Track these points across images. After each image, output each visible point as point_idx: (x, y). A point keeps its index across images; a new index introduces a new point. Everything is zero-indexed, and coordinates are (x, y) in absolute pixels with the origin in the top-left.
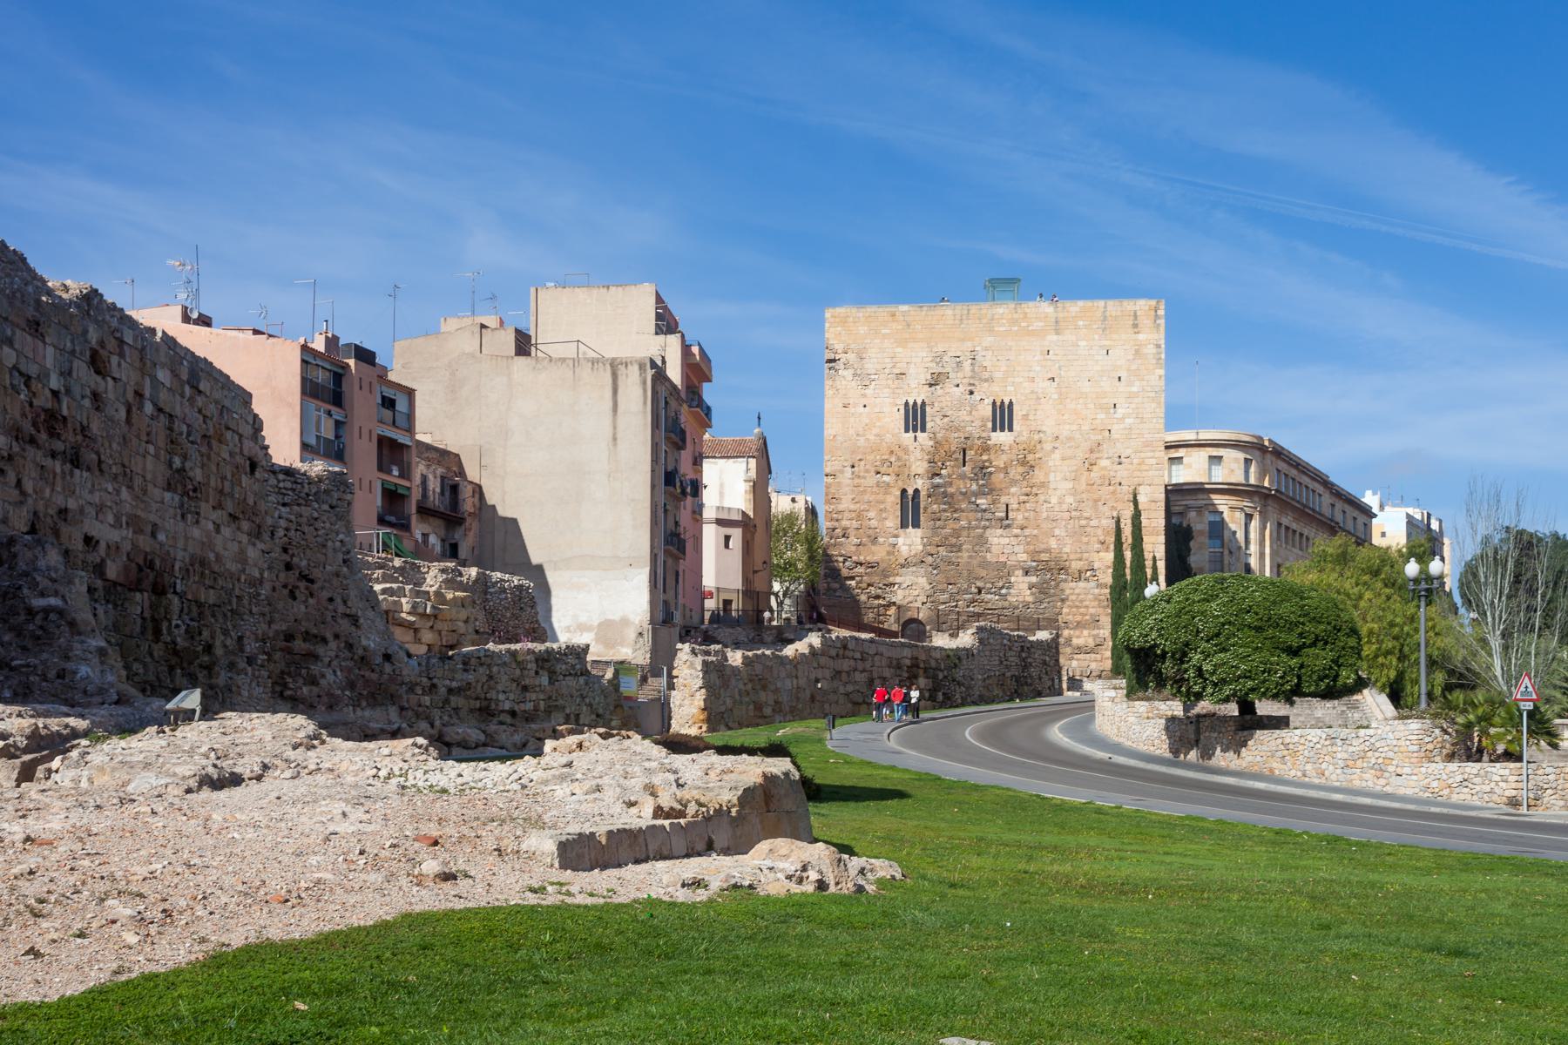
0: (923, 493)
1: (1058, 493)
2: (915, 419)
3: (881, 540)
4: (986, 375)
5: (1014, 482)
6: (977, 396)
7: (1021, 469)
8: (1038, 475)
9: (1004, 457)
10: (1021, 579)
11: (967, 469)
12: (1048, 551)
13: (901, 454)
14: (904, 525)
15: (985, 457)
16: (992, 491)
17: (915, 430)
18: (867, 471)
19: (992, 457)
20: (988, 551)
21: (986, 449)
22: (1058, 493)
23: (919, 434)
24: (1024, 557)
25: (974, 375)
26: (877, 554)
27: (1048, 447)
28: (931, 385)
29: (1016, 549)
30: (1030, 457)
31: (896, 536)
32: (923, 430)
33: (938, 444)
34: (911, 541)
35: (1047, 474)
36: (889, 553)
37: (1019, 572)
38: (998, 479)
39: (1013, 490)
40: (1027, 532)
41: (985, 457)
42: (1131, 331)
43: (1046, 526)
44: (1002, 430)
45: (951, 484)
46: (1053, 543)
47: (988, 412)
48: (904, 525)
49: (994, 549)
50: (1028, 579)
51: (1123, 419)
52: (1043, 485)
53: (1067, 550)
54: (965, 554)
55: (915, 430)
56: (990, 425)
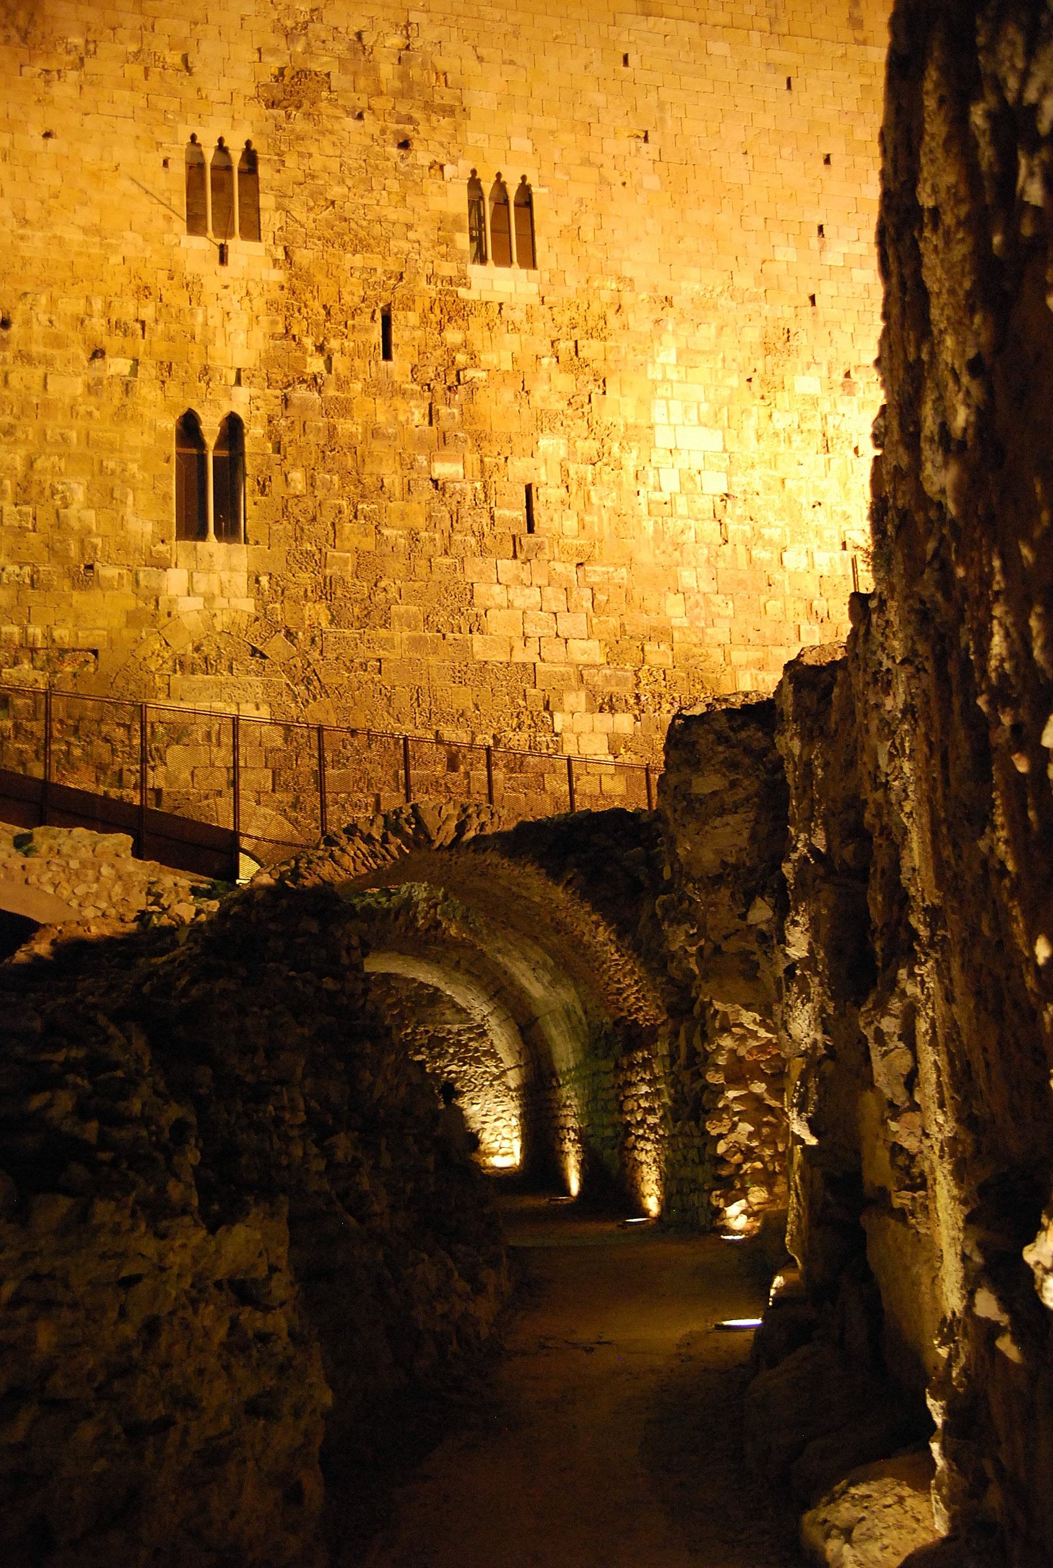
0: (254, 433)
1: (682, 461)
2: (221, 186)
3: (108, 572)
4: (446, 97)
5: (543, 422)
6: (422, 156)
7: (564, 382)
8: (619, 407)
9: (512, 341)
10: (585, 721)
11: (399, 366)
12: (663, 634)
13: (178, 299)
14: (192, 527)
15: (453, 336)
16: (479, 440)
17: (225, 230)
18: (57, 341)
19: (477, 335)
20: (477, 627)
21: (453, 310)
22: (682, 461)
23: (237, 246)
24: (588, 651)
25: (407, 90)
26: (93, 618)
27: (640, 320)
28: (273, 104)
29: (565, 625)
30: (591, 349)
31: (162, 565)
32: (252, 231)
33: (298, 282)
34: (212, 584)
35: (643, 403)
36: (133, 619)
37: (576, 700)
38: (496, 405)
39: (546, 443)
40: (596, 573)
41: (453, 336)
42: (847, 34)
43: (644, 557)
44: (504, 259)
45: (345, 409)
46: (675, 611)
47: (458, 202)
48: (192, 527)
49: (495, 621)
50: (605, 722)
51: (847, 268)
52: (640, 434)
53: (720, 633)
54: (401, 634)
55: (225, 230)
56: (463, 241)
